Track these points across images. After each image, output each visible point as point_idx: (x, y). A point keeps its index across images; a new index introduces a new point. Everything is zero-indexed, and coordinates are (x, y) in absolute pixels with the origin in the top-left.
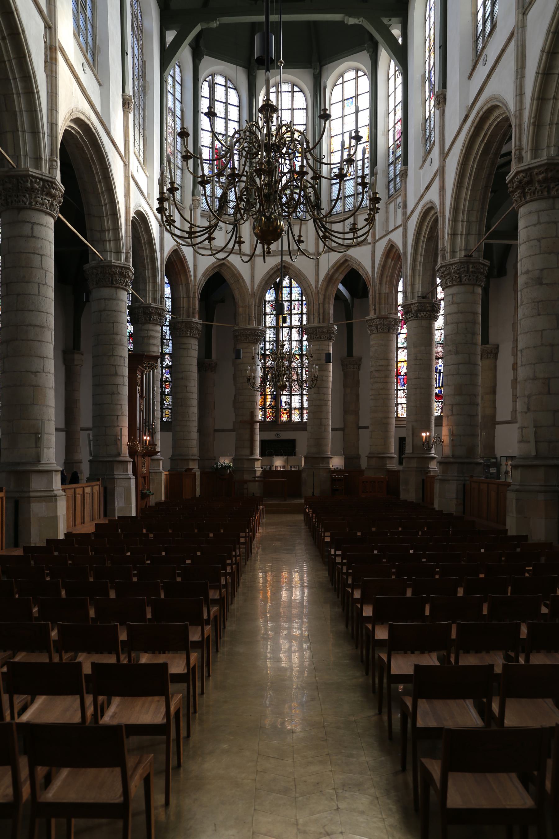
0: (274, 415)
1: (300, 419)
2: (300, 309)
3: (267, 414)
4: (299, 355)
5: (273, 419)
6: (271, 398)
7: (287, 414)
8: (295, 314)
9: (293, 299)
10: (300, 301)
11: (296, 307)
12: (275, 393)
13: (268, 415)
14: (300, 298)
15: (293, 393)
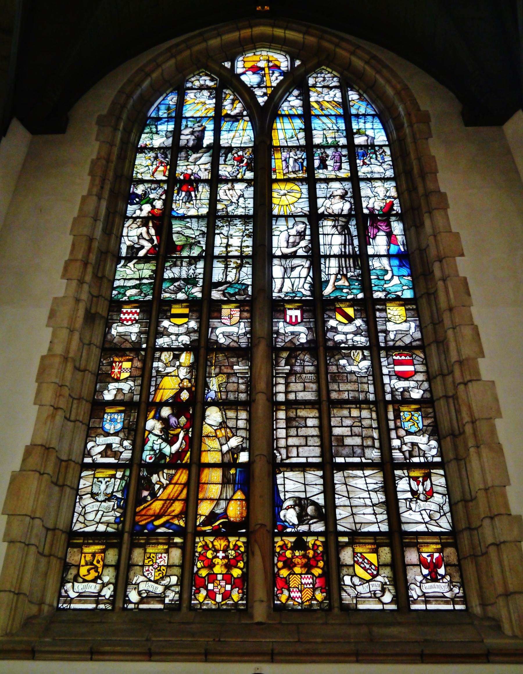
0: (236, 573)
1: (387, 598)
2: (346, 166)
3: (199, 565)
4: (353, 303)
5: (227, 595)
6: (225, 482)
7: (308, 567)
8: (327, 181)
9: (317, 140)
10: (343, 147)
11: (330, 162)
12: (244, 457)
13: (204, 573)
14: (343, 141)
15: (340, 460)
